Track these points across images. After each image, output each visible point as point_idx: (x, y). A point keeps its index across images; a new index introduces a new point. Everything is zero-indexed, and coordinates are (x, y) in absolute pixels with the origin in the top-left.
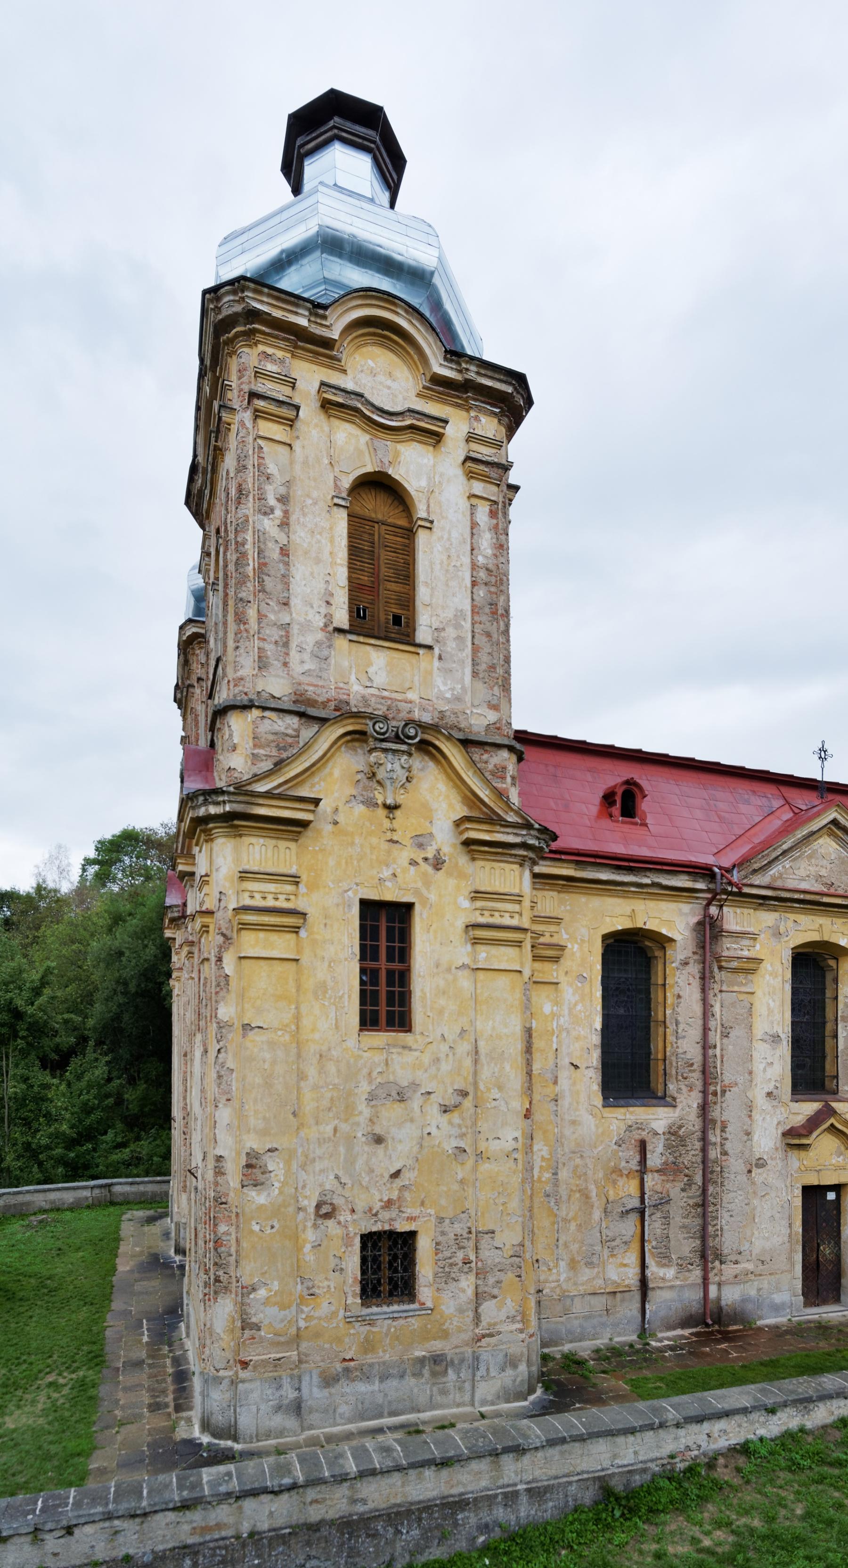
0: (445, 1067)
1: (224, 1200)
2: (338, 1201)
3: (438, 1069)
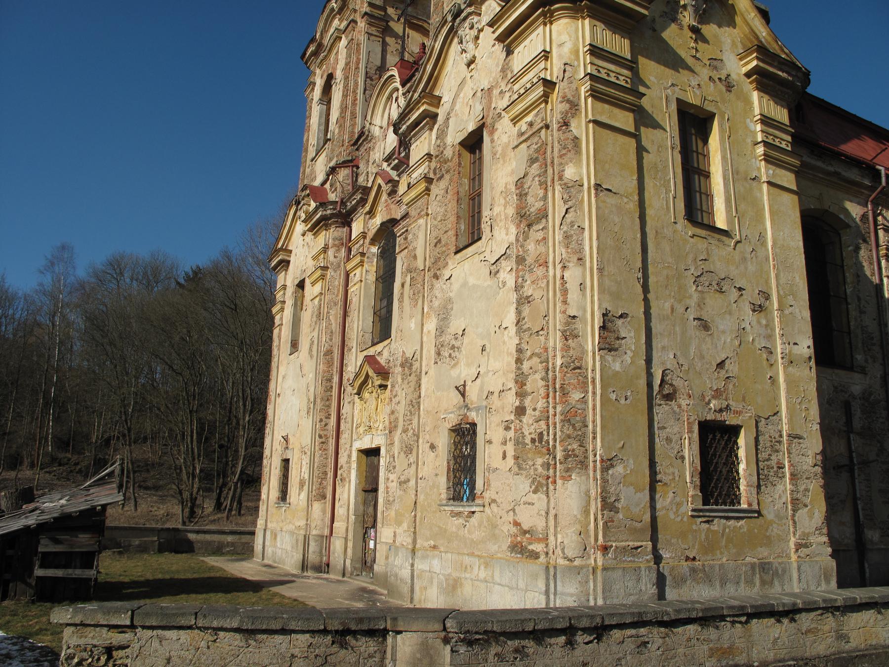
0: (751, 268)
1: (578, 364)
2: (678, 383)
3: (746, 268)
